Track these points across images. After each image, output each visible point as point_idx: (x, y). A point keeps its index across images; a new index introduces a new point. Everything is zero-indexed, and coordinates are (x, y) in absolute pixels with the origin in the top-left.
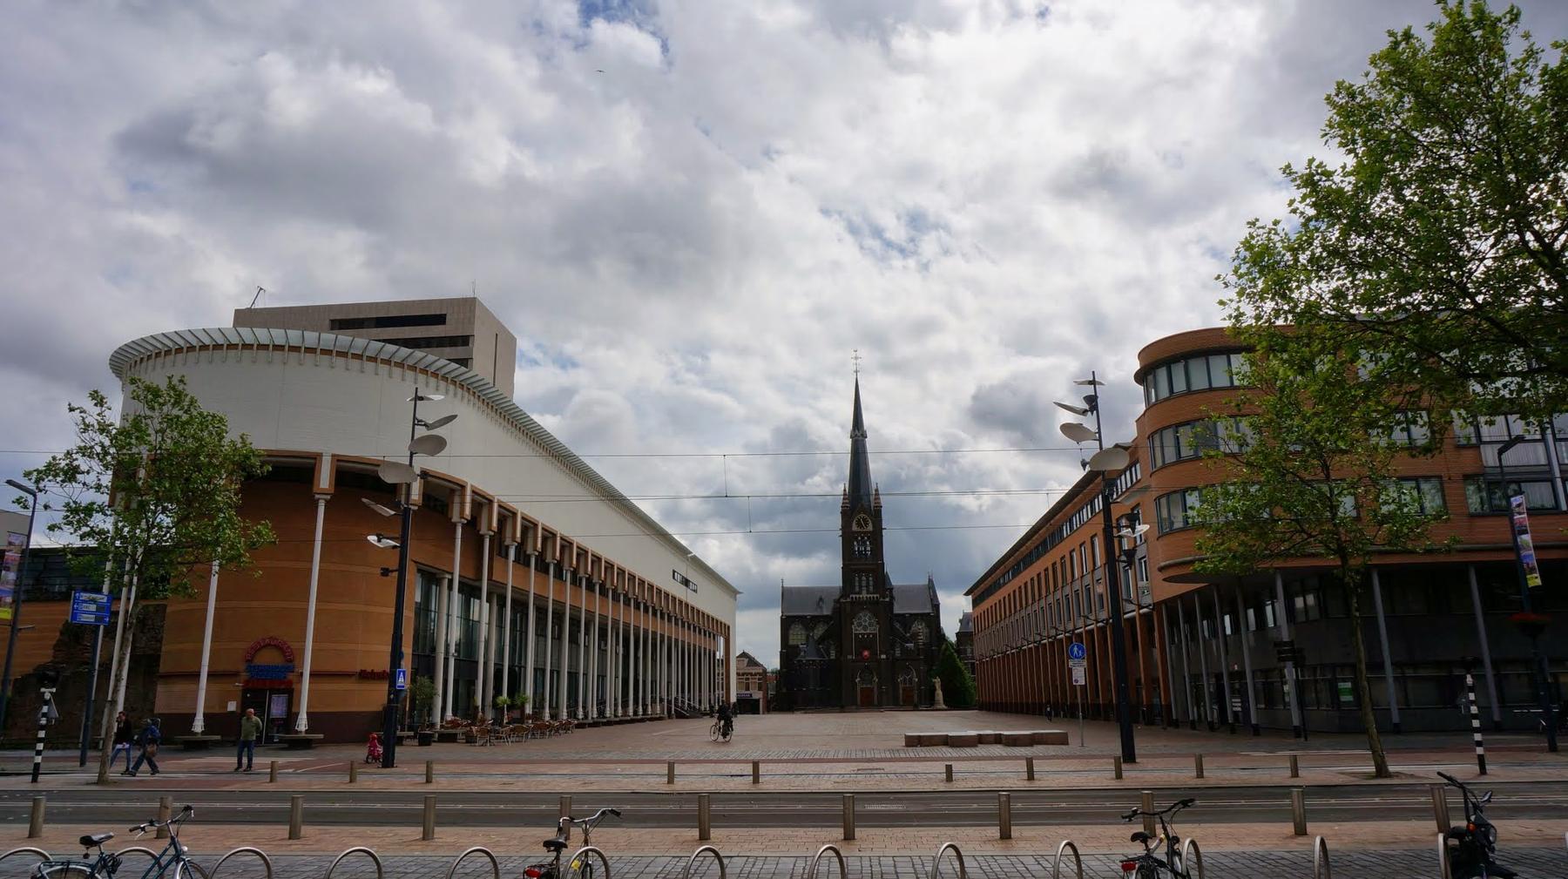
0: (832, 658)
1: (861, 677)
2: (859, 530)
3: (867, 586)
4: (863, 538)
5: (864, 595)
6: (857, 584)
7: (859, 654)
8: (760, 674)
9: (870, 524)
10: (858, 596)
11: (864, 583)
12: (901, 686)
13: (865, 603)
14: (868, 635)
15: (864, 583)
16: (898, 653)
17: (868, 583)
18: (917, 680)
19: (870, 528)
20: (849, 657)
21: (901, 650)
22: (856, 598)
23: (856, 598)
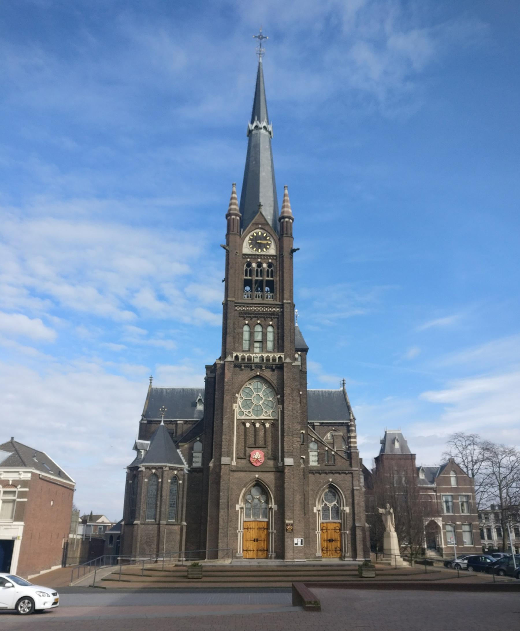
0: (195, 465)
1: (246, 501)
2: (253, 252)
3: (263, 342)
4: (259, 265)
5: (257, 355)
6: (246, 336)
7: (245, 456)
8: (24, 483)
9: (273, 246)
10: (246, 355)
12: (320, 520)
16: (313, 461)
17: (264, 335)
19: (272, 251)
21: (319, 455)
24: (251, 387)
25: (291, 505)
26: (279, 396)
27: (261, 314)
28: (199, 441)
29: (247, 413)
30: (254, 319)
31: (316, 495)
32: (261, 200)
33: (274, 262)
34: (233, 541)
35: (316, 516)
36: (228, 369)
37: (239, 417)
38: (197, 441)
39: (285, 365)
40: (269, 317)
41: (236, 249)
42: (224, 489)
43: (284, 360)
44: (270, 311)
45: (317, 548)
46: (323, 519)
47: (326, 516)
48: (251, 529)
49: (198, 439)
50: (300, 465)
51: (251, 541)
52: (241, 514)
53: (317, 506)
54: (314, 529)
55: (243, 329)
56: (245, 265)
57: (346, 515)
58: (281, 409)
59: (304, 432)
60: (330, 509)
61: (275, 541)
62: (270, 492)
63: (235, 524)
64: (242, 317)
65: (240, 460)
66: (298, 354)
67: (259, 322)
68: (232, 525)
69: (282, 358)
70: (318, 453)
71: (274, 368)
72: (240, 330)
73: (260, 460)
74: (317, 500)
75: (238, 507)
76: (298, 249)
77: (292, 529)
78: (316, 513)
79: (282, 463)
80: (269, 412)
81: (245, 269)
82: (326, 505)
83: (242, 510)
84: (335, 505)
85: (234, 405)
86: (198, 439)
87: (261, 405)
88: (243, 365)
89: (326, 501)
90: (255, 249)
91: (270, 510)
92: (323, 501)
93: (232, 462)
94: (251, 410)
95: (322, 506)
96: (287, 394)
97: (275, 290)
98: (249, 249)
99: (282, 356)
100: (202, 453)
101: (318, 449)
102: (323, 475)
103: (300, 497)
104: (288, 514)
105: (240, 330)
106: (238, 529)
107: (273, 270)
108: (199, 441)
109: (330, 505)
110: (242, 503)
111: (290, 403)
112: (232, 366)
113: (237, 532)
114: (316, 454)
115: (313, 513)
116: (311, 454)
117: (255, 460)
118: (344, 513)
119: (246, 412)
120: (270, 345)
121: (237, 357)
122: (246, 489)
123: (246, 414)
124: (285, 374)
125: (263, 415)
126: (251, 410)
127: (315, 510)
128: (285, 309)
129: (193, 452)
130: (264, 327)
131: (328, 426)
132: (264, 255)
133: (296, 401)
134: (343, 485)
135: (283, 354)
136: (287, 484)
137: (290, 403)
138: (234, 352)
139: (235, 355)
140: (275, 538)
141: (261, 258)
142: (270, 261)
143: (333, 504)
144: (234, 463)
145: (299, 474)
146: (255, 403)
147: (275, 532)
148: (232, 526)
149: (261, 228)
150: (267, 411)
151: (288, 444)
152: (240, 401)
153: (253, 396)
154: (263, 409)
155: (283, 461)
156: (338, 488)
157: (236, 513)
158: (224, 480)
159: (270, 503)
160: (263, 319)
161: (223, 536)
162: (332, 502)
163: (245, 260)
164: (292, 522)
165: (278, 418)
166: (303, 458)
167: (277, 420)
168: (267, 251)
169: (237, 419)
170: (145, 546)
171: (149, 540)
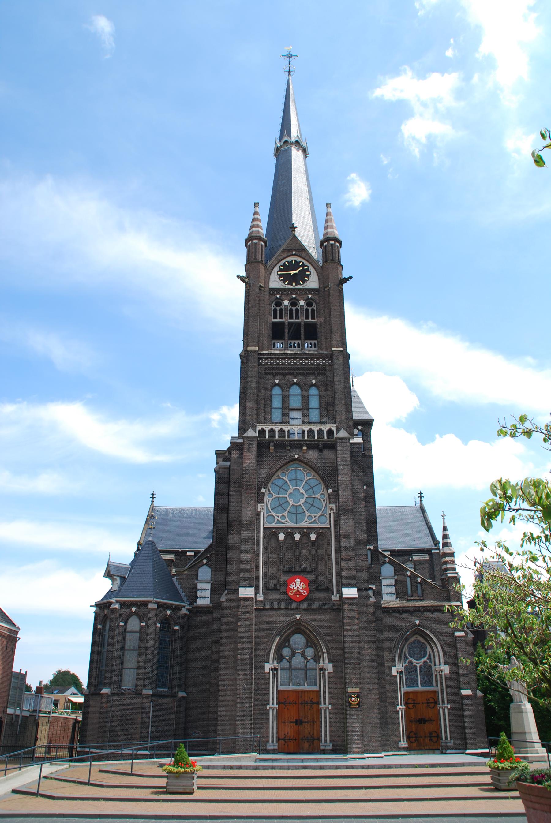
0: (200, 602)
4: (294, 303)
6: (277, 402)
11: (295, 402)
12: (402, 689)
13: (297, 445)
14: (305, 532)
15: (295, 402)
17: (305, 400)
18: (446, 669)
19: (313, 282)
20: (246, 592)
22: (272, 432)
23: (272, 432)
24: (286, 478)
25: (357, 663)
26: (330, 491)
27: (298, 369)
28: (206, 564)
29: (279, 519)
30: (288, 377)
31: (396, 648)
32: (295, 220)
33: (315, 297)
35: (397, 682)
36: (248, 450)
37: (267, 525)
38: (204, 565)
39: (338, 441)
40: (311, 374)
41: (259, 282)
42: (243, 638)
43: (337, 433)
44: (313, 364)
45: (400, 733)
46: (407, 686)
47: (412, 682)
49: (205, 561)
50: (369, 598)
51: (292, 724)
52: (273, 678)
53: (397, 665)
54: (394, 703)
55: (271, 391)
56: (273, 304)
57: (445, 678)
58: (335, 511)
59: (372, 547)
60: (418, 668)
61: (331, 725)
63: (264, 696)
64: (269, 374)
65: (270, 593)
66: (358, 429)
67: (295, 380)
68: (258, 696)
69: (333, 431)
70: (396, 580)
71: (321, 446)
72: (268, 393)
73: (302, 591)
74: (397, 655)
75: (268, 667)
76: (351, 278)
78: (396, 676)
79: (338, 595)
80: (315, 517)
81: (273, 308)
82: (411, 663)
83: (275, 672)
84: (425, 662)
85: (260, 506)
86: (205, 561)
87: (302, 505)
88: (272, 443)
89: (410, 656)
90: (286, 283)
91: (322, 672)
92: (406, 658)
93: (258, 595)
94: (285, 514)
95: (404, 665)
96: (343, 486)
97: (319, 336)
98: (279, 282)
99: (334, 429)
100: (211, 584)
101: (395, 575)
102: (405, 616)
103: (370, 650)
104: (351, 677)
105: (268, 393)
106: (268, 704)
107: (315, 309)
108: (206, 564)
109: (418, 664)
110: (275, 661)
111: (348, 500)
112: (255, 444)
113: (268, 708)
114: (393, 582)
115: (392, 676)
116: (384, 582)
117: (294, 591)
118: (441, 676)
119: (278, 516)
120: (314, 415)
121: (262, 432)
123: (277, 520)
124: (339, 455)
125: (305, 521)
126: (285, 514)
127: (394, 673)
128: (335, 361)
129: (196, 581)
130: (305, 388)
131: (402, 555)
132: (300, 289)
133: (358, 496)
134: (438, 630)
135: (335, 425)
136: (348, 628)
137: (348, 500)
138: (257, 425)
139: (258, 428)
140: (330, 718)
141: (296, 294)
142: (310, 296)
143: (423, 660)
144: (260, 597)
145: (366, 613)
146: (292, 502)
147: (330, 707)
148: (258, 699)
149: (295, 255)
150: (312, 515)
151: (346, 564)
152: (269, 500)
153: (290, 491)
154: (305, 512)
155: (340, 592)
156: (432, 636)
157: (264, 676)
158: (244, 623)
159: (321, 661)
160: (302, 377)
161: (244, 716)
162: (420, 659)
163: (274, 297)
164: (357, 690)
165: (330, 525)
166: (372, 589)
167: (329, 529)
168: (305, 284)
169: (264, 528)
170: (118, 730)
171: (124, 720)
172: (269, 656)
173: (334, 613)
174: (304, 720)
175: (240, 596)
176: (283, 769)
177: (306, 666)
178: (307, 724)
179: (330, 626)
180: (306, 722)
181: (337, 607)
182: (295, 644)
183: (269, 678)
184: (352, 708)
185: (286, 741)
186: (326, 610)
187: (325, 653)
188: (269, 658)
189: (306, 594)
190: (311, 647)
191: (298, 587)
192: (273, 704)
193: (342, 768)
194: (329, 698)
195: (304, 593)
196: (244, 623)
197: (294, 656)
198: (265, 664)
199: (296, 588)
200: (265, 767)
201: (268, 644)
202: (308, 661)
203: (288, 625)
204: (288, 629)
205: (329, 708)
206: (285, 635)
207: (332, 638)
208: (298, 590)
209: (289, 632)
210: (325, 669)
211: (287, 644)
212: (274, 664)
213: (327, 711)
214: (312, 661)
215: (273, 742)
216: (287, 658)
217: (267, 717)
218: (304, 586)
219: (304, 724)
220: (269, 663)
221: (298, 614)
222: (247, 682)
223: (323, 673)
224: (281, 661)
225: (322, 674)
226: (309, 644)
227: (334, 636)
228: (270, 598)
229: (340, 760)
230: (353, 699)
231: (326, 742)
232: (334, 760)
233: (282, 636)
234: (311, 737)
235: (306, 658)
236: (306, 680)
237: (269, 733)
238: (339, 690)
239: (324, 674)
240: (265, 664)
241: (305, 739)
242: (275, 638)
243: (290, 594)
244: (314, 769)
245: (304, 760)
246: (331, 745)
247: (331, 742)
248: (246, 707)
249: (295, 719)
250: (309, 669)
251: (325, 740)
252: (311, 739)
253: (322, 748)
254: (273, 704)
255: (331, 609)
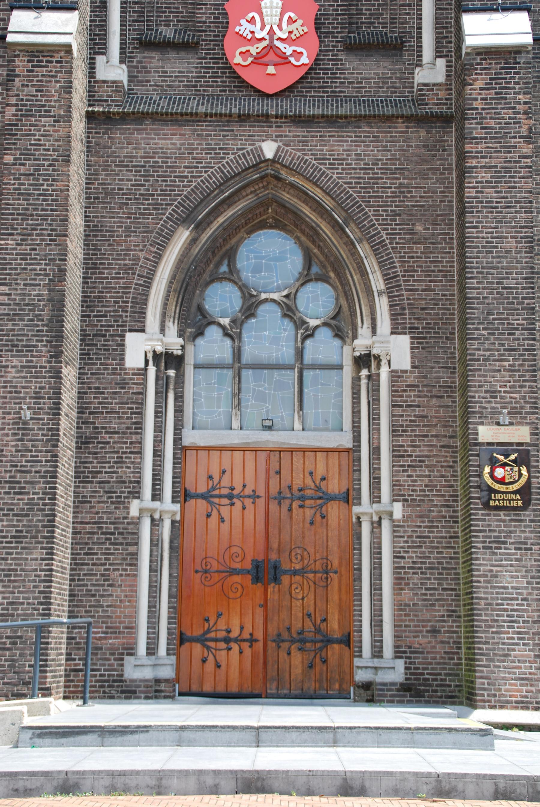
25: (519, 321)
34: (105, 577)
42: (25, 216)
48: (230, 497)
51: (237, 579)
62: (363, 250)
63: (120, 462)
68: (95, 465)
73: (288, 50)
77: (528, 483)
83: (172, 373)
91: (364, 372)
93: (100, 60)
106: (137, 494)
110: (172, 328)
122: (193, 241)
136: (484, 176)
140: (397, 556)
157: (123, 385)
159: (364, 331)
161: (18, 537)
172: (145, 302)
173: (423, 133)
174: (285, 566)
175: (10, 38)
176: (126, 790)
177: (300, 353)
178: (298, 578)
179: (401, 186)
180: (295, 573)
181: (435, 109)
182: (257, 270)
183: (143, 393)
184: (497, 508)
185: (212, 644)
186: (389, 119)
187: (380, 293)
188: (143, 314)
189: (304, 60)
190: (323, 278)
191: (271, 32)
192: (156, 496)
193: (471, 788)
194: (394, 474)
195: (298, 55)
196: (27, 154)
197: (253, 315)
198: (128, 335)
199: (264, 34)
200: (20, 784)
201: (141, 255)
202: (310, 334)
203: (227, 180)
204: (228, 202)
205: (391, 514)
206: (215, 226)
207: (412, 232)
208: (271, 47)
209: (230, 213)
210: (378, 358)
211: (224, 268)
212: (167, 340)
213: (386, 525)
214: (324, 334)
215: (152, 650)
216: (225, 321)
217: (131, 549)
218: (298, 28)
219: (285, 579)
220: (143, 331)
221: (268, 137)
222: (37, 396)
223: (369, 377)
224: (200, 333)
225: (364, 382)
226: (315, 269)
227: (419, 228)
228: (154, 78)
229: (449, 737)
230: (499, 472)
231: (378, 653)
232: (418, 737)
233: (200, 227)
234: (318, 630)
235: (299, 324)
236: (301, 408)
237: (134, 615)
238: (435, 441)
239: (373, 379)
240: (128, 335)
241: (292, 641)
242: (172, 233)
243: (238, 60)
244: (310, 792)
245: (264, 735)
246: (400, 664)
247: (398, 654)
248: (31, 504)
249: (249, 558)
250: (313, 367)
251: (373, 647)
252: (314, 642)
253: (361, 676)
254: (156, 496)
255: (408, 118)
